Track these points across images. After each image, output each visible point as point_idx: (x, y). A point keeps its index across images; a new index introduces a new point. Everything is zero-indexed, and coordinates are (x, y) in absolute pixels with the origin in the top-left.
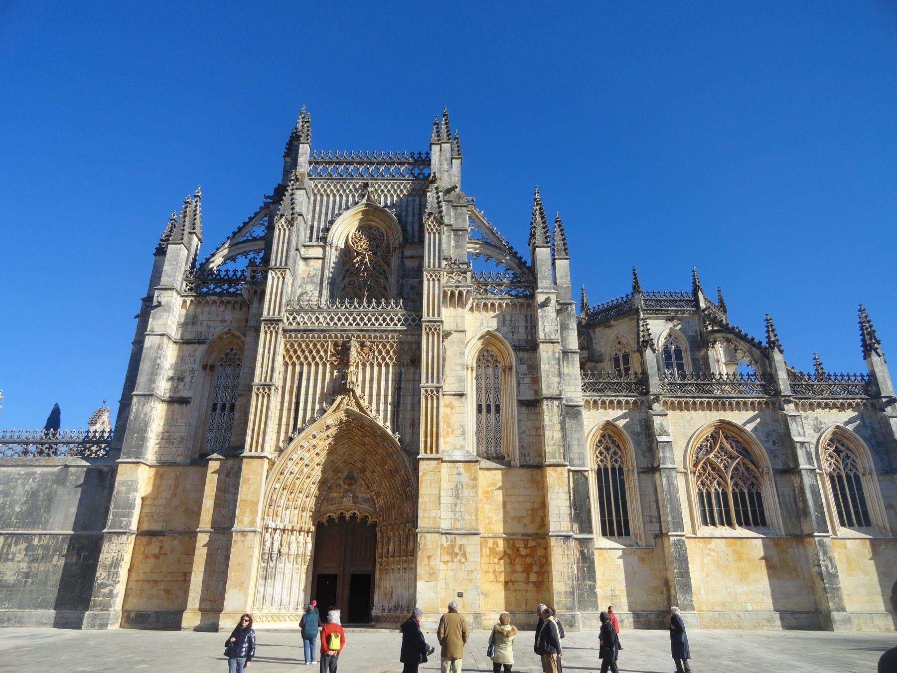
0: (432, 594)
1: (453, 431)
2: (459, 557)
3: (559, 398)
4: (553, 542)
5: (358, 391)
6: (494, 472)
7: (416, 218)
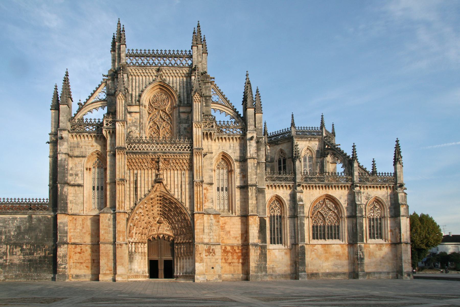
0: (202, 268)
1: (208, 200)
2: (212, 254)
3: (255, 185)
4: (251, 247)
5: (165, 182)
6: (225, 218)
7: (185, 90)
